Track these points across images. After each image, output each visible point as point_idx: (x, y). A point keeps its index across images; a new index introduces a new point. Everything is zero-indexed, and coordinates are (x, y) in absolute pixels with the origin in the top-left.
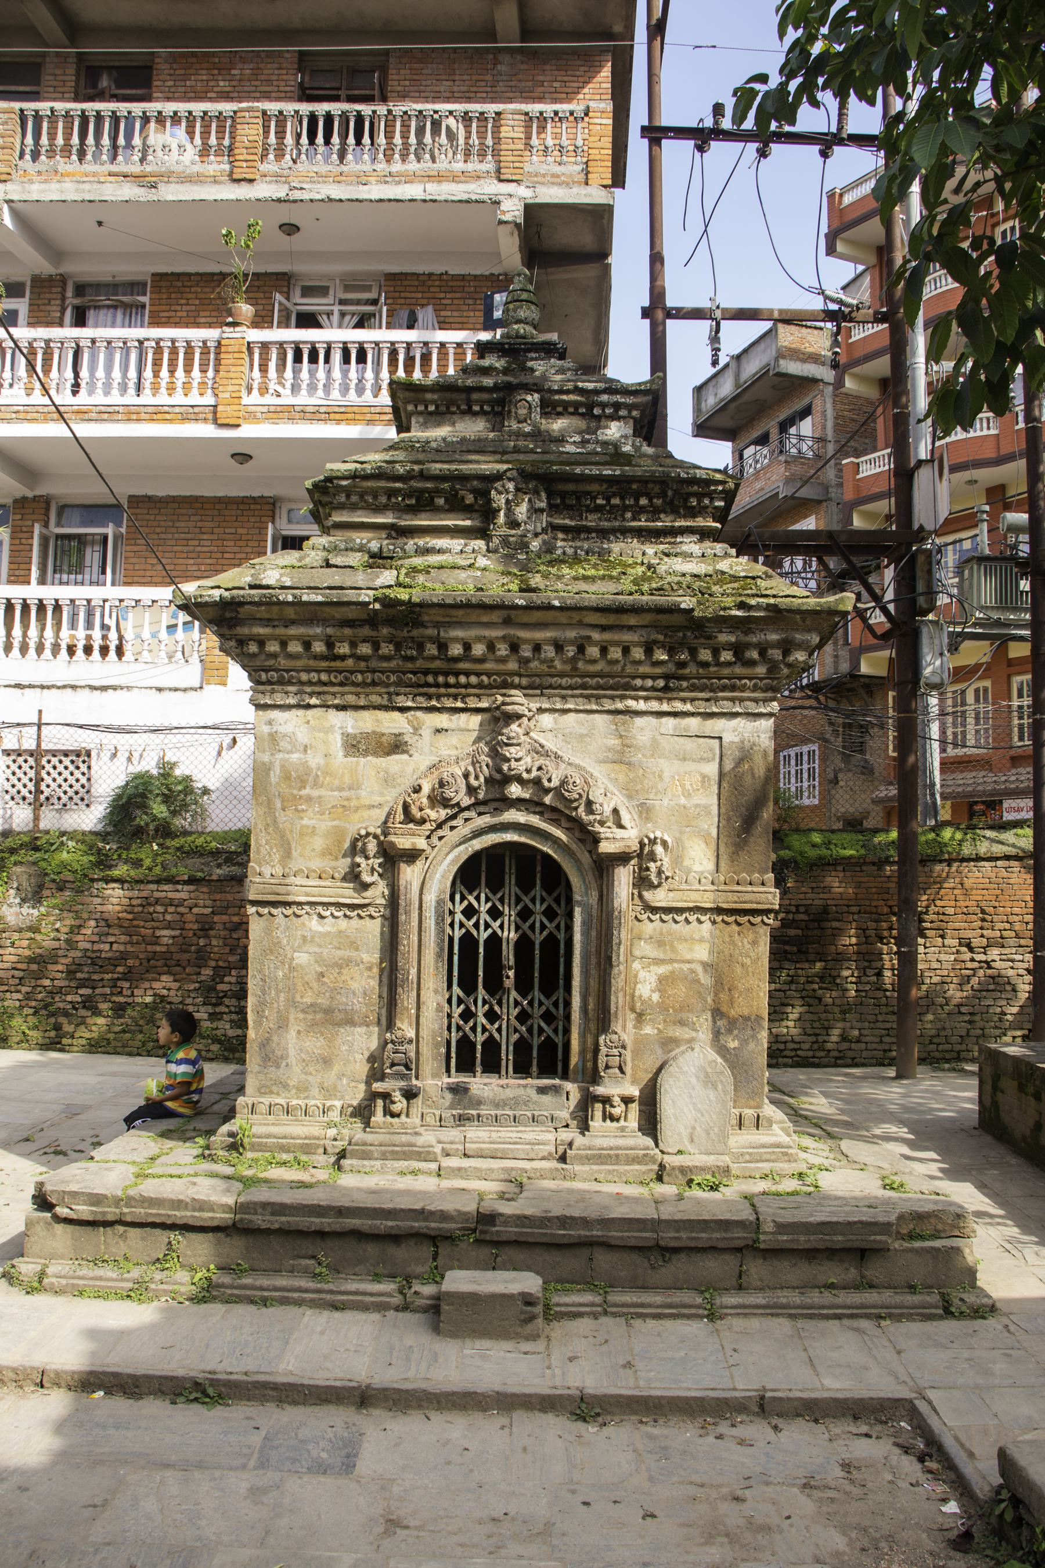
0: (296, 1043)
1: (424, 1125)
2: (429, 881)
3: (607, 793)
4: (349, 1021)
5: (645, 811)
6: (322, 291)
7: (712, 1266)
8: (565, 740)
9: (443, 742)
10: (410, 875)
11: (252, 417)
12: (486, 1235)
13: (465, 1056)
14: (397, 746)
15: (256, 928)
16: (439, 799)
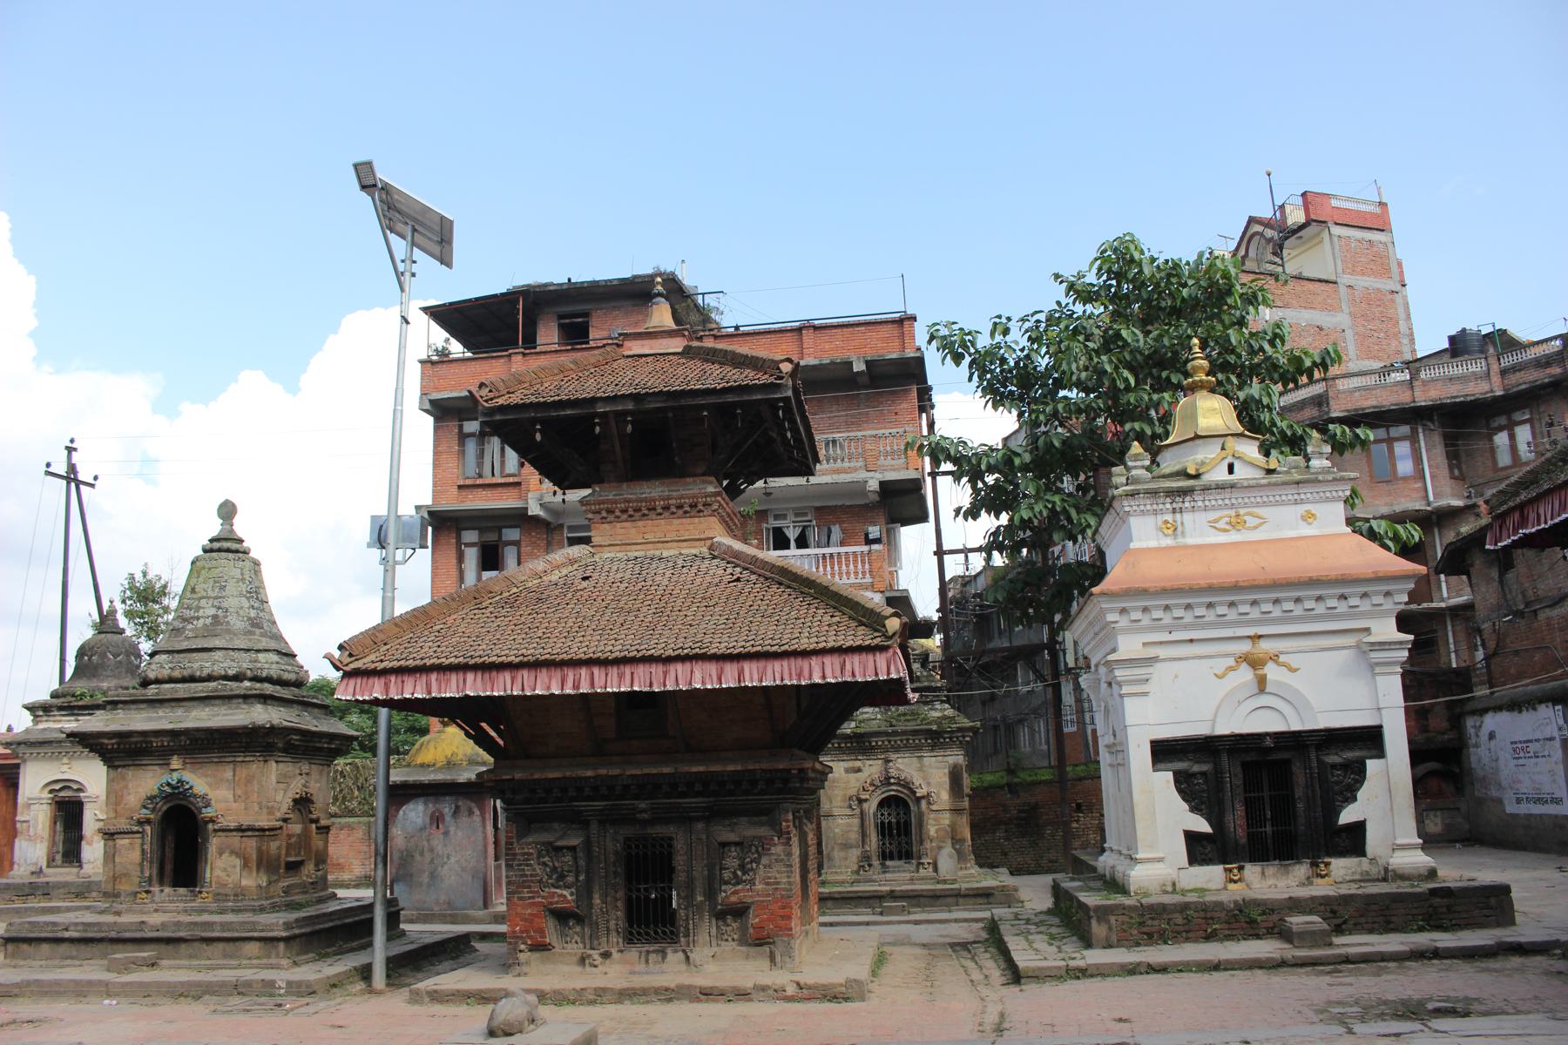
0: (837, 854)
1: (875, 872)
2: (871, 806)
5: (929, 784)
6: (784, 517)
7: (950, 900)
8: (905, 765)
10: (865, 805)
12: (893, 895)
13: (885, 856)
14: (859, 770)
15: (824, 824)
16: (872, 784)
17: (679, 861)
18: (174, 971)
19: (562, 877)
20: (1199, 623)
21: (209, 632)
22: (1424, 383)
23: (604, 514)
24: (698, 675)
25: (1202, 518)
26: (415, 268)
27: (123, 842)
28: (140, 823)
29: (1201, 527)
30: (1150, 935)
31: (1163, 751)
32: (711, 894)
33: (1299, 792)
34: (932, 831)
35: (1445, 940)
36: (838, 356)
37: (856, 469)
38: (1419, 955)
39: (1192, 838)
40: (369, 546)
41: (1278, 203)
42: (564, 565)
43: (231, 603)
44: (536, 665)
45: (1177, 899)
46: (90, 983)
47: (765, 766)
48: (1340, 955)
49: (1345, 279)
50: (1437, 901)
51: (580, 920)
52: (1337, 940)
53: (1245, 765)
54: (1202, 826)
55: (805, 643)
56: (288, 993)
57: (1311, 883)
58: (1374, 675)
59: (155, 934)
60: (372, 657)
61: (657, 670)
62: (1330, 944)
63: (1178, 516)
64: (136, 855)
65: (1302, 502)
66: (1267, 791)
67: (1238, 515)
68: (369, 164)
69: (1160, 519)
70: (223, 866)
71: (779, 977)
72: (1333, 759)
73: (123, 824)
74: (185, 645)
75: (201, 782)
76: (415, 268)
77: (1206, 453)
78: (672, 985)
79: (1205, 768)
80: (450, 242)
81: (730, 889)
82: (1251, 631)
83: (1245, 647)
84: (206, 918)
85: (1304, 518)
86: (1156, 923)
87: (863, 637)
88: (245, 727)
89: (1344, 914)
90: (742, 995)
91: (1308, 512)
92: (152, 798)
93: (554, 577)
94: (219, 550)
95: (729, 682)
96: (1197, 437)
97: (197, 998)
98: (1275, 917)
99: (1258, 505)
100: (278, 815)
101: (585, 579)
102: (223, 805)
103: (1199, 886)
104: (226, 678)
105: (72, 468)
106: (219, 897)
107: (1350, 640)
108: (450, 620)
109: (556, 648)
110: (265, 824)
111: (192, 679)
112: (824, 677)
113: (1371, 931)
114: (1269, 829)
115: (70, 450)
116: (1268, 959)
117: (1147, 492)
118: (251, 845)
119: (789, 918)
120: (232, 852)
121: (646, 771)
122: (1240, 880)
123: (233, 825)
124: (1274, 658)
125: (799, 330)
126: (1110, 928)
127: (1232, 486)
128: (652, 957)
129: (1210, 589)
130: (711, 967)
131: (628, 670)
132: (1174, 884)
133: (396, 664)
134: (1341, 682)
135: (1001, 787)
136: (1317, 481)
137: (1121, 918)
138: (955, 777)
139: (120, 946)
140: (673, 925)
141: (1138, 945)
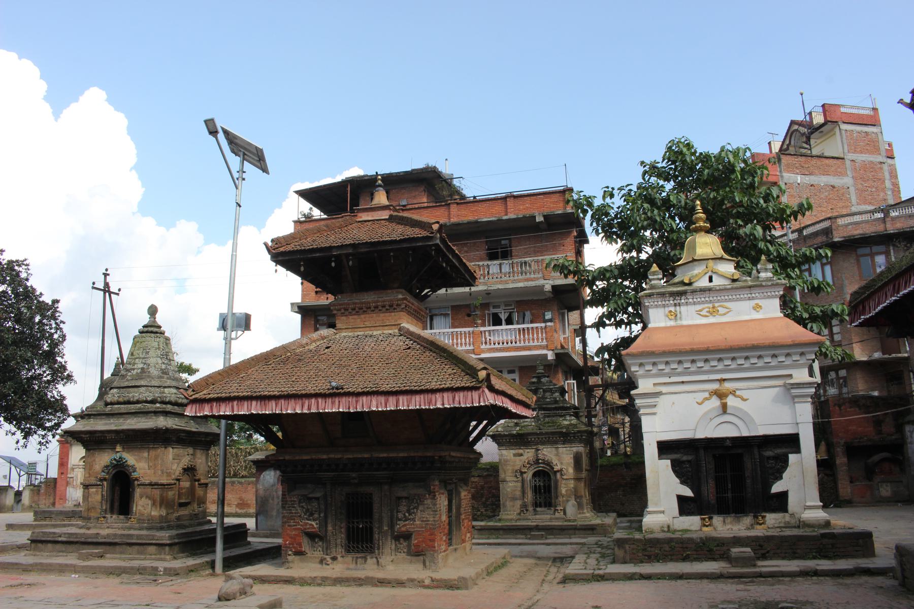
1: (529, 515)
2: (529, 476)
3: (555, 461)
4: (516, 499)
5: (562, 463)
6: (498, 307)
7: (570, 532)
8: (547, 452)
9: (529, 454)
10: (525, 475)
11: (483, 351)
12: (537, 528)
13: (536, 505)
14: (521, 455)
17: (376, 507)
18: (111, 561)
19: (312, 514)
20: (686, 372)
21: (139, 377)
22: (894, 219)
23: (343, 311)
24: (374, 403)
25: (692, 309)
26: (244, 176)
27: (93, 490)
28: (101, 480)
29: (691, 315)
30: (649, 557)
31: (665, 448)
32: (392, 526)
33: (748, 473)
34: (563, 491)
35: (825, 565)
36: (528, 213)
37: (537, 279)
38: (805, 573)
39: (681, 499)
40: (218, 330)
41: (807, 111)
42: (318, 340)
43: (152, 361)
44: (288, 397)
45: (669, 535)
46: (66, 565)
47: (420, 454)
48: (756, 572)
49: (849, 156)
50: (825, 541)
51: (321, 539)
52: (760, 563)
53: (714, 456)
54: (688, 492)
55: (434, 385)
56: (164, 574)
57: (753, 528)
58: (794, 403)
59: (103, 540)
60: (205, 392)
61: (352, 400)
62: (755, 566)
63: (678, 308)
64: (99, 497)
65: (753, 298)
66: (729, 472)
67: (714, 307)
68: (212, 120)
69: (667, 309)
70: (142, 505)
71: (424, 575)
72: (769, 453)
73: (93, 481)
74: (126, 384)
75: (130, 459)
76: (244, 176)
77: (698, 270)
78: (363, 577)
79: (690, 458)
80: (264, 160)
81: (401, 523)
82: (718, 376)
83: (715, 386)
84: (132, 532)
85: (754, 308)
86: (653, 549)
87: (466, 382)
88: (152, 429)
89: (765, 547)
90: (400, 583)
91: (757, 304)
92: (107, 467)
93: (312, 346)
94: (147, 332)
95: (391, 407)
96: (694, 260)
97: (119, 575)
98: (725, 548)
99: (726, 301)
100: (173, 477)
101: (327, 348)
102: (142, 471)
103: (685, 527)
104: (147, 402)
105: (107, 285)
106: (140, 521)
107: (780, 382)
108: (250, 371)
109: (299, 388)
110: (165, 482)
111: (129, 402)
112: (443, 404)
113: (783, 558)
114: (730, 495)
115: (106, 275)
116: (713, 573)
117: (658, 294)
118: (157, 493)
119: (434, 541)
120: (147, 497)
121: (355, 456)
122: (710, 525)
123: (147, 482)
124: (733, 393)
125: (505, 198)
126: (625, 552)
127: (710, 290)
128: (359, 560)
129: (693, 352)
130: (391, 567)
131: (337, 400)
132: (669, 527)
133: (216, 396)
134: (768, 407)
135: (620, 465)
136: (761, 286)
137: (632, 546)
138: (577, 459)
139: (86, 546)
140: (371, 541)
141: (642, 562)
